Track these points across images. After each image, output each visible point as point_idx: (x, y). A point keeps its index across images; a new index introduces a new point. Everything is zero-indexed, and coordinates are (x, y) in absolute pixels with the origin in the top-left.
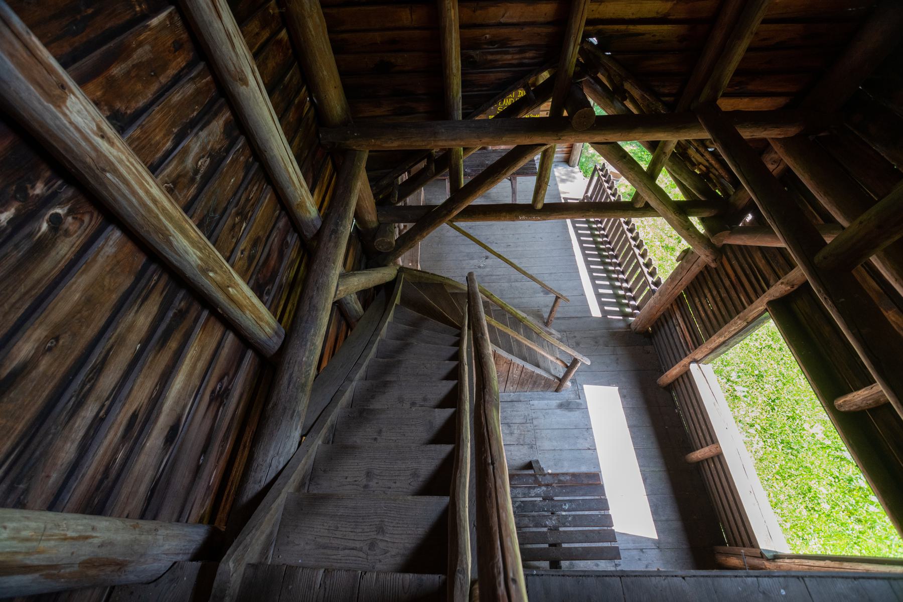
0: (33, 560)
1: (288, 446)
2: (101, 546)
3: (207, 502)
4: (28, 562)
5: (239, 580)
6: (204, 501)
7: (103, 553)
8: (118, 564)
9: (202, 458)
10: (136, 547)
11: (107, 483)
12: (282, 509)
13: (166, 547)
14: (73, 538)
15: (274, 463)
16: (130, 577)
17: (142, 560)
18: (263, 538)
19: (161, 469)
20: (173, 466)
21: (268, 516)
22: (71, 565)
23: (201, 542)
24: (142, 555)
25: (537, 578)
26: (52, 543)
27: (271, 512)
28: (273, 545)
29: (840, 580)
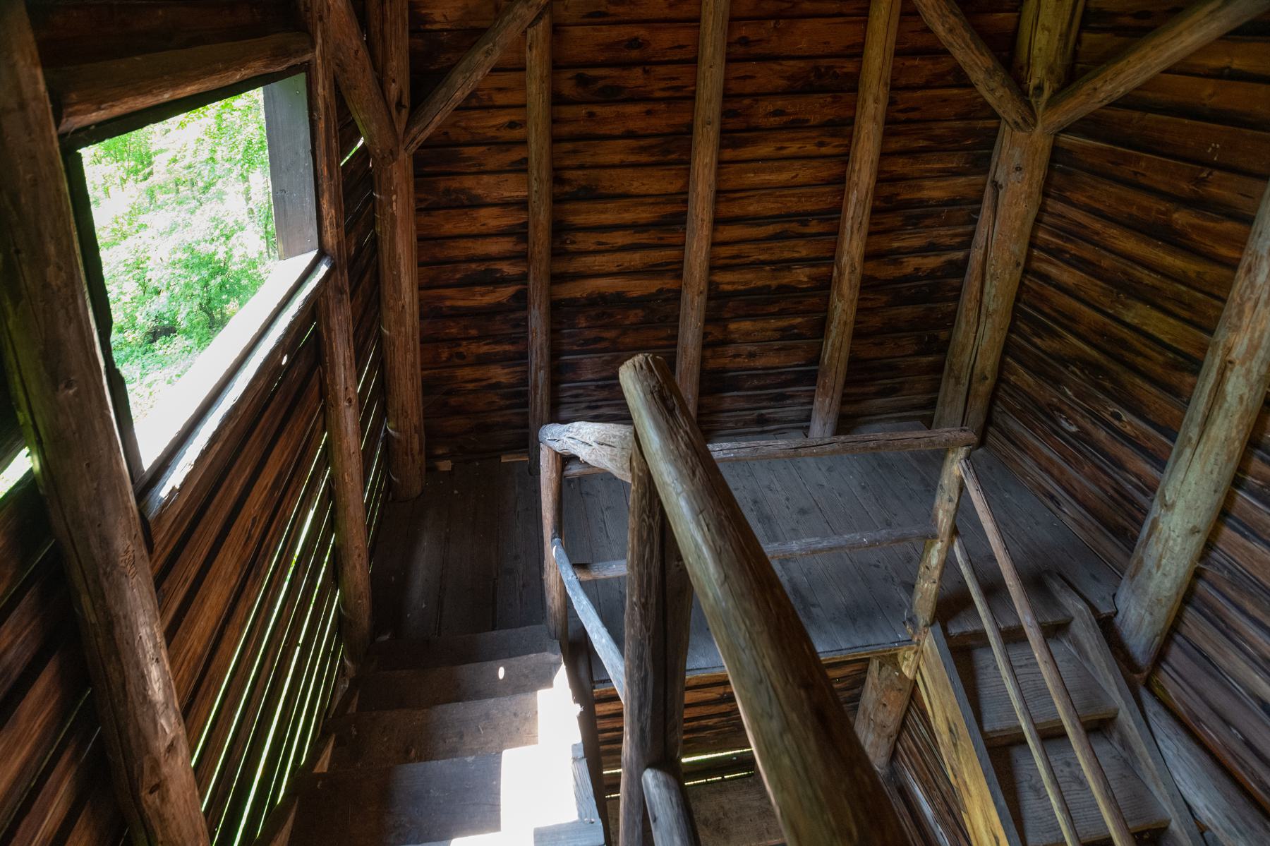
0: (1153, 539)
1: (1185, 775)
2: (1149, 572)
3: (1182, 708)
4: (1153, 536)
5: (1065, 604)
6: (1184, 704)
7: (1144, 570)
8: (1134, 575)
9: (1240, 736)
10: (1140, 590)
11: (1232, 634)
12: (1106, 688)
13: (1133, 611)
14: (1160, 560)
15: (1168, 742)
16: (1125, 580)
17: (1130, 591)
18: (1087, 647)
19: (1229, 678)
20: (1229, 690)
21: (1104, 664)
22: (1144, 552)
23: (1126, 641)
24: (1133, 591)
25: (893, 640)
26: (1160, 550)
27: (1106, 671)
28: (1078, 656)
29: (703, 666)
